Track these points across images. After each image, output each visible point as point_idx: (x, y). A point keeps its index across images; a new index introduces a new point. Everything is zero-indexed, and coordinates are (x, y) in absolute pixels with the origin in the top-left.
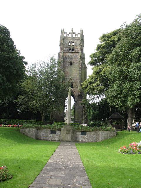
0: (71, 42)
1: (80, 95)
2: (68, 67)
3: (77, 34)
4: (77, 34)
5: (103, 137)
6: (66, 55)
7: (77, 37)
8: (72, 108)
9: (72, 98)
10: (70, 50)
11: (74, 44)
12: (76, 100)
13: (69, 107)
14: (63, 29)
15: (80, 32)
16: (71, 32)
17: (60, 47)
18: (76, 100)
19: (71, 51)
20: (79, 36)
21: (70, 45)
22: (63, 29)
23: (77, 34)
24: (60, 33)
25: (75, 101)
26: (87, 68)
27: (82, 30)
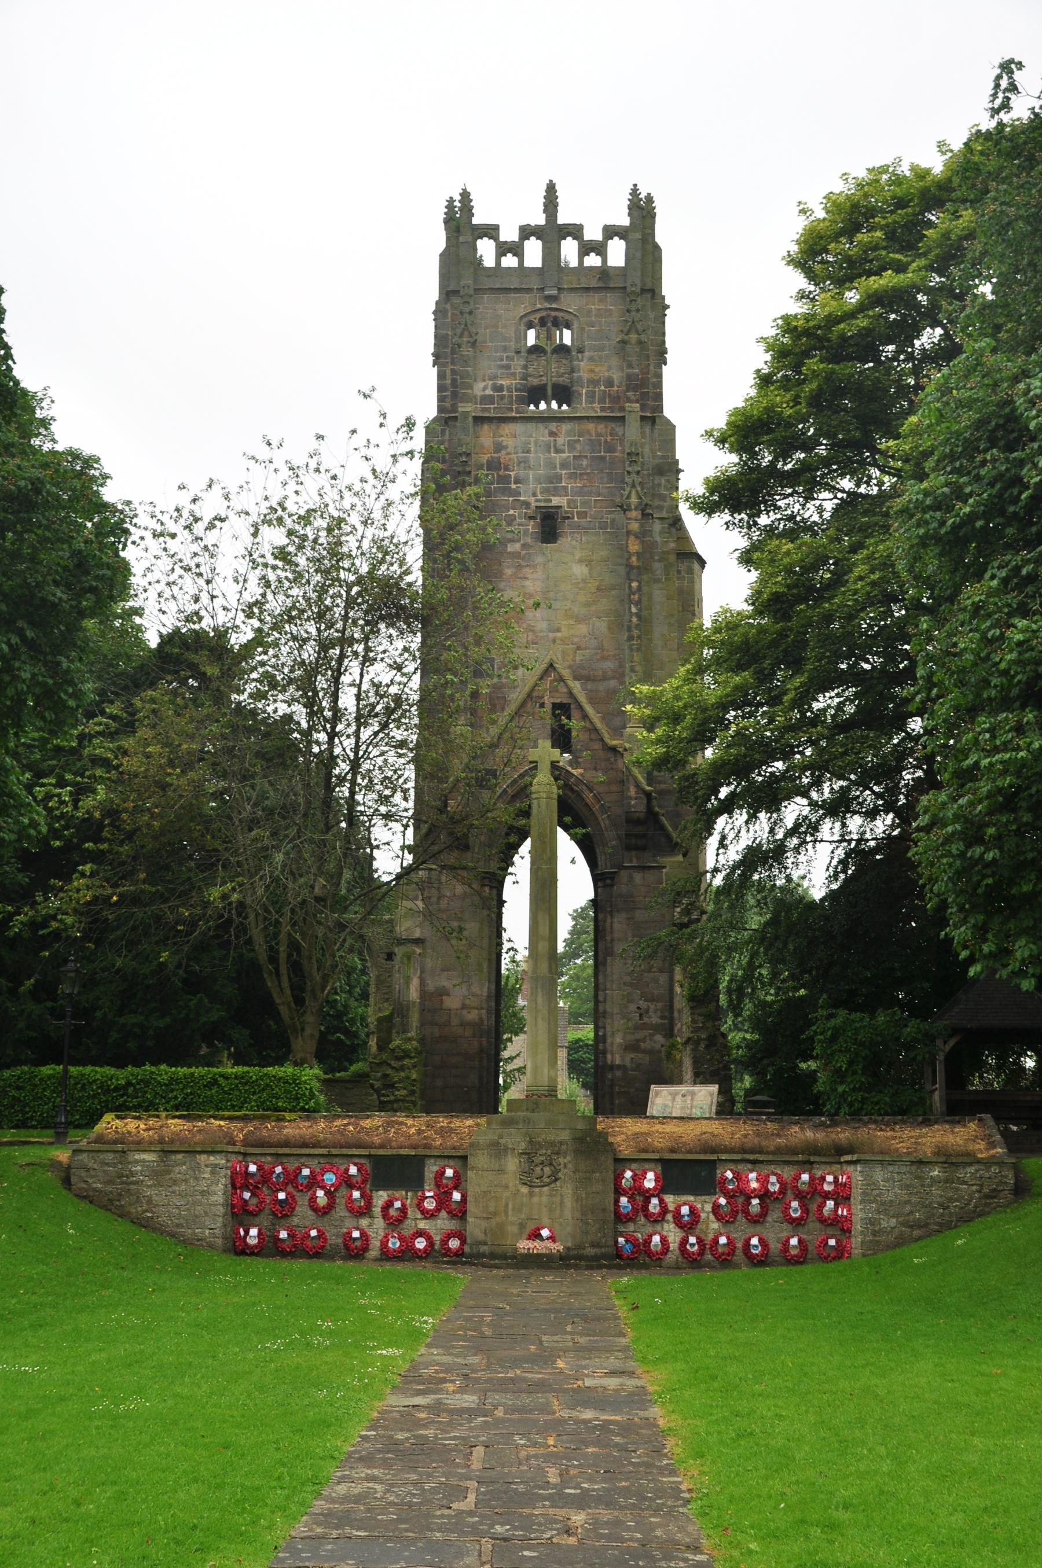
0: (543, 322)
1: (638, 822)
2: (516, 555)
3: (598, 236)
4: (593, 233)
5: (884, 1207)
6: (499, 447)
7: (604, 272)
8: (568, 943)
9: (566, 846)
10: (536, 394)
11: (567, 340)
12: (603, 868)
13: (544, 930)
14: (465, 195)
15: (623, 220)
16: (540, 220)
17: (441, 376)
18: (603, 868)
19: (543, 406)
20: (617, 253)
21: (536, 349)
22: (465, 195)
23: (598, 236)
24: (438, 240)
25: (597, 878)
26: (702, 563)
27: (649, 199)
